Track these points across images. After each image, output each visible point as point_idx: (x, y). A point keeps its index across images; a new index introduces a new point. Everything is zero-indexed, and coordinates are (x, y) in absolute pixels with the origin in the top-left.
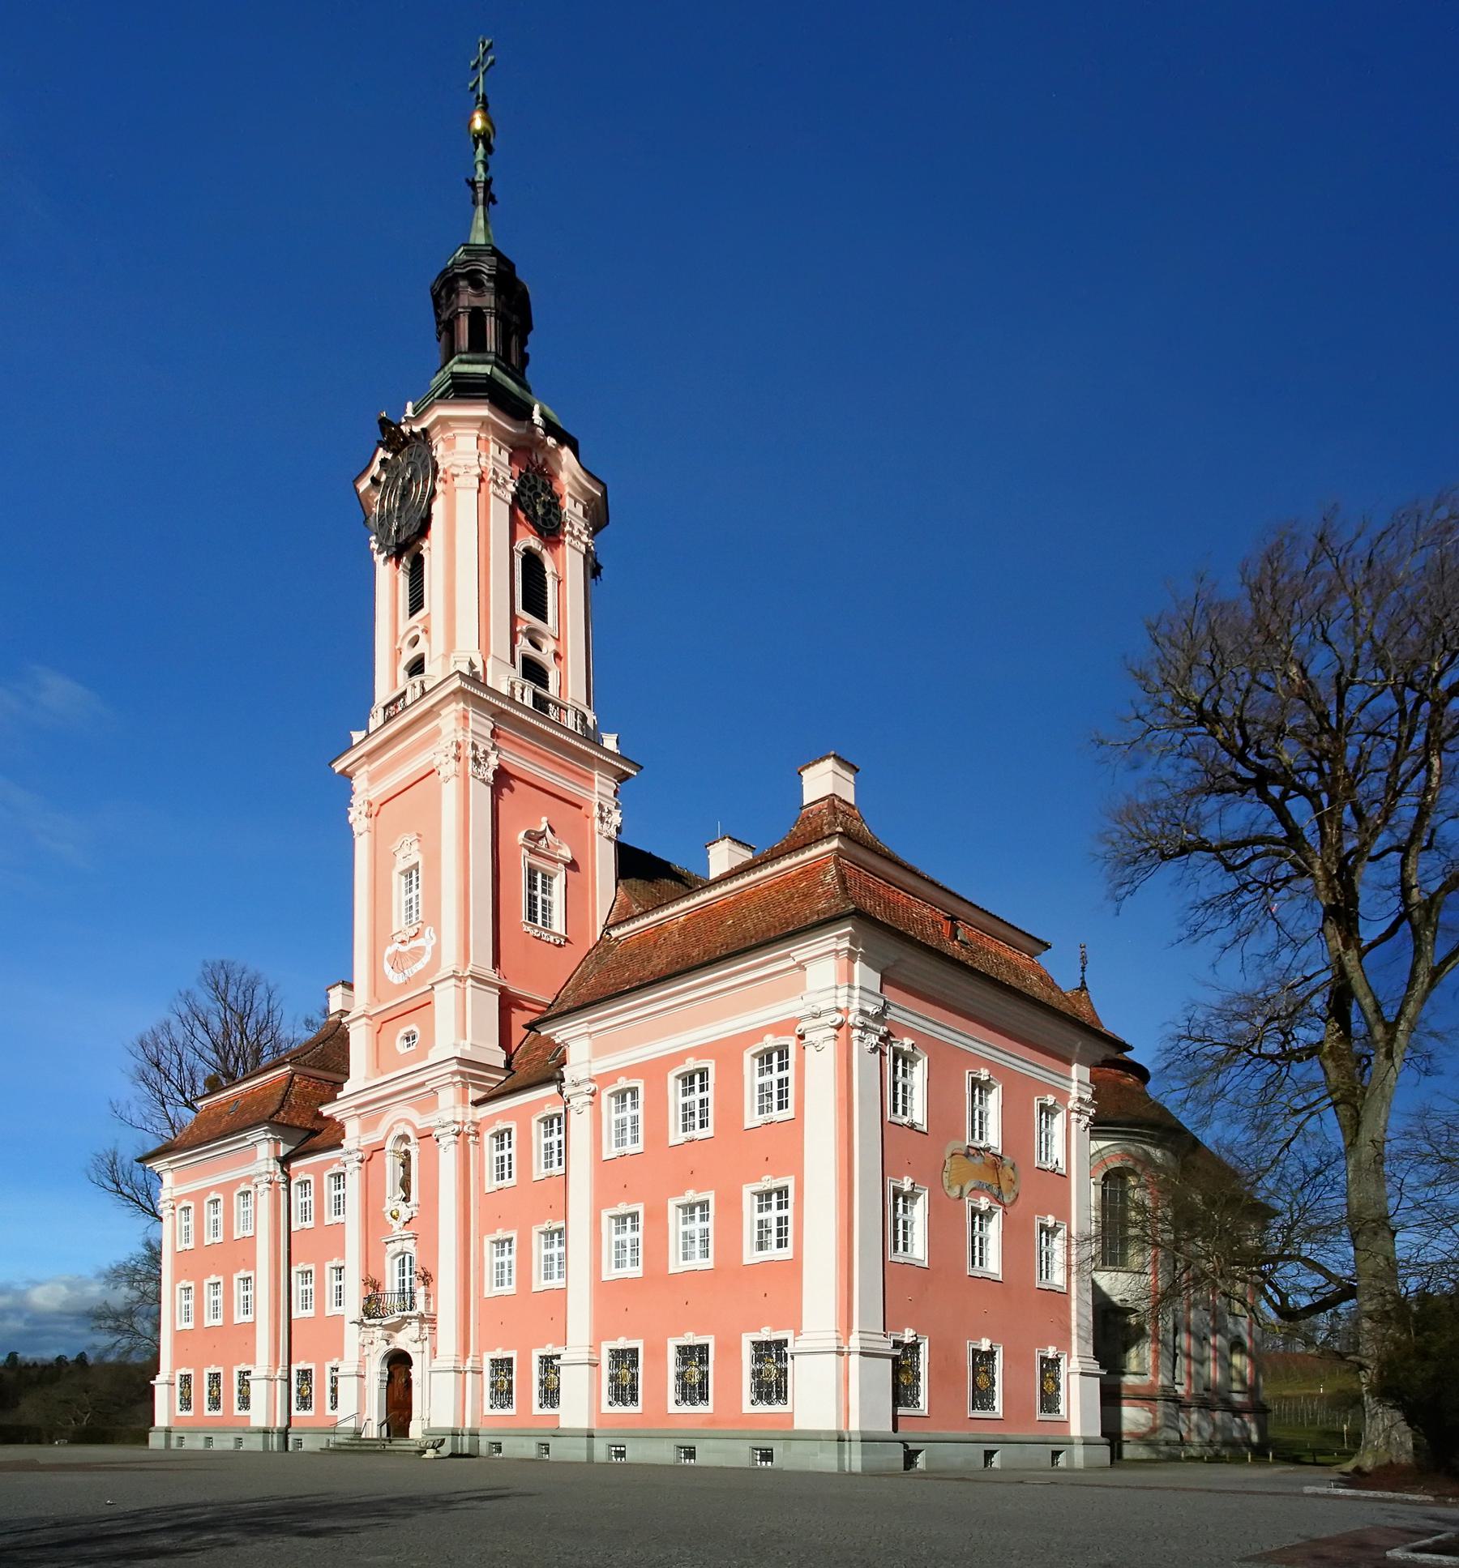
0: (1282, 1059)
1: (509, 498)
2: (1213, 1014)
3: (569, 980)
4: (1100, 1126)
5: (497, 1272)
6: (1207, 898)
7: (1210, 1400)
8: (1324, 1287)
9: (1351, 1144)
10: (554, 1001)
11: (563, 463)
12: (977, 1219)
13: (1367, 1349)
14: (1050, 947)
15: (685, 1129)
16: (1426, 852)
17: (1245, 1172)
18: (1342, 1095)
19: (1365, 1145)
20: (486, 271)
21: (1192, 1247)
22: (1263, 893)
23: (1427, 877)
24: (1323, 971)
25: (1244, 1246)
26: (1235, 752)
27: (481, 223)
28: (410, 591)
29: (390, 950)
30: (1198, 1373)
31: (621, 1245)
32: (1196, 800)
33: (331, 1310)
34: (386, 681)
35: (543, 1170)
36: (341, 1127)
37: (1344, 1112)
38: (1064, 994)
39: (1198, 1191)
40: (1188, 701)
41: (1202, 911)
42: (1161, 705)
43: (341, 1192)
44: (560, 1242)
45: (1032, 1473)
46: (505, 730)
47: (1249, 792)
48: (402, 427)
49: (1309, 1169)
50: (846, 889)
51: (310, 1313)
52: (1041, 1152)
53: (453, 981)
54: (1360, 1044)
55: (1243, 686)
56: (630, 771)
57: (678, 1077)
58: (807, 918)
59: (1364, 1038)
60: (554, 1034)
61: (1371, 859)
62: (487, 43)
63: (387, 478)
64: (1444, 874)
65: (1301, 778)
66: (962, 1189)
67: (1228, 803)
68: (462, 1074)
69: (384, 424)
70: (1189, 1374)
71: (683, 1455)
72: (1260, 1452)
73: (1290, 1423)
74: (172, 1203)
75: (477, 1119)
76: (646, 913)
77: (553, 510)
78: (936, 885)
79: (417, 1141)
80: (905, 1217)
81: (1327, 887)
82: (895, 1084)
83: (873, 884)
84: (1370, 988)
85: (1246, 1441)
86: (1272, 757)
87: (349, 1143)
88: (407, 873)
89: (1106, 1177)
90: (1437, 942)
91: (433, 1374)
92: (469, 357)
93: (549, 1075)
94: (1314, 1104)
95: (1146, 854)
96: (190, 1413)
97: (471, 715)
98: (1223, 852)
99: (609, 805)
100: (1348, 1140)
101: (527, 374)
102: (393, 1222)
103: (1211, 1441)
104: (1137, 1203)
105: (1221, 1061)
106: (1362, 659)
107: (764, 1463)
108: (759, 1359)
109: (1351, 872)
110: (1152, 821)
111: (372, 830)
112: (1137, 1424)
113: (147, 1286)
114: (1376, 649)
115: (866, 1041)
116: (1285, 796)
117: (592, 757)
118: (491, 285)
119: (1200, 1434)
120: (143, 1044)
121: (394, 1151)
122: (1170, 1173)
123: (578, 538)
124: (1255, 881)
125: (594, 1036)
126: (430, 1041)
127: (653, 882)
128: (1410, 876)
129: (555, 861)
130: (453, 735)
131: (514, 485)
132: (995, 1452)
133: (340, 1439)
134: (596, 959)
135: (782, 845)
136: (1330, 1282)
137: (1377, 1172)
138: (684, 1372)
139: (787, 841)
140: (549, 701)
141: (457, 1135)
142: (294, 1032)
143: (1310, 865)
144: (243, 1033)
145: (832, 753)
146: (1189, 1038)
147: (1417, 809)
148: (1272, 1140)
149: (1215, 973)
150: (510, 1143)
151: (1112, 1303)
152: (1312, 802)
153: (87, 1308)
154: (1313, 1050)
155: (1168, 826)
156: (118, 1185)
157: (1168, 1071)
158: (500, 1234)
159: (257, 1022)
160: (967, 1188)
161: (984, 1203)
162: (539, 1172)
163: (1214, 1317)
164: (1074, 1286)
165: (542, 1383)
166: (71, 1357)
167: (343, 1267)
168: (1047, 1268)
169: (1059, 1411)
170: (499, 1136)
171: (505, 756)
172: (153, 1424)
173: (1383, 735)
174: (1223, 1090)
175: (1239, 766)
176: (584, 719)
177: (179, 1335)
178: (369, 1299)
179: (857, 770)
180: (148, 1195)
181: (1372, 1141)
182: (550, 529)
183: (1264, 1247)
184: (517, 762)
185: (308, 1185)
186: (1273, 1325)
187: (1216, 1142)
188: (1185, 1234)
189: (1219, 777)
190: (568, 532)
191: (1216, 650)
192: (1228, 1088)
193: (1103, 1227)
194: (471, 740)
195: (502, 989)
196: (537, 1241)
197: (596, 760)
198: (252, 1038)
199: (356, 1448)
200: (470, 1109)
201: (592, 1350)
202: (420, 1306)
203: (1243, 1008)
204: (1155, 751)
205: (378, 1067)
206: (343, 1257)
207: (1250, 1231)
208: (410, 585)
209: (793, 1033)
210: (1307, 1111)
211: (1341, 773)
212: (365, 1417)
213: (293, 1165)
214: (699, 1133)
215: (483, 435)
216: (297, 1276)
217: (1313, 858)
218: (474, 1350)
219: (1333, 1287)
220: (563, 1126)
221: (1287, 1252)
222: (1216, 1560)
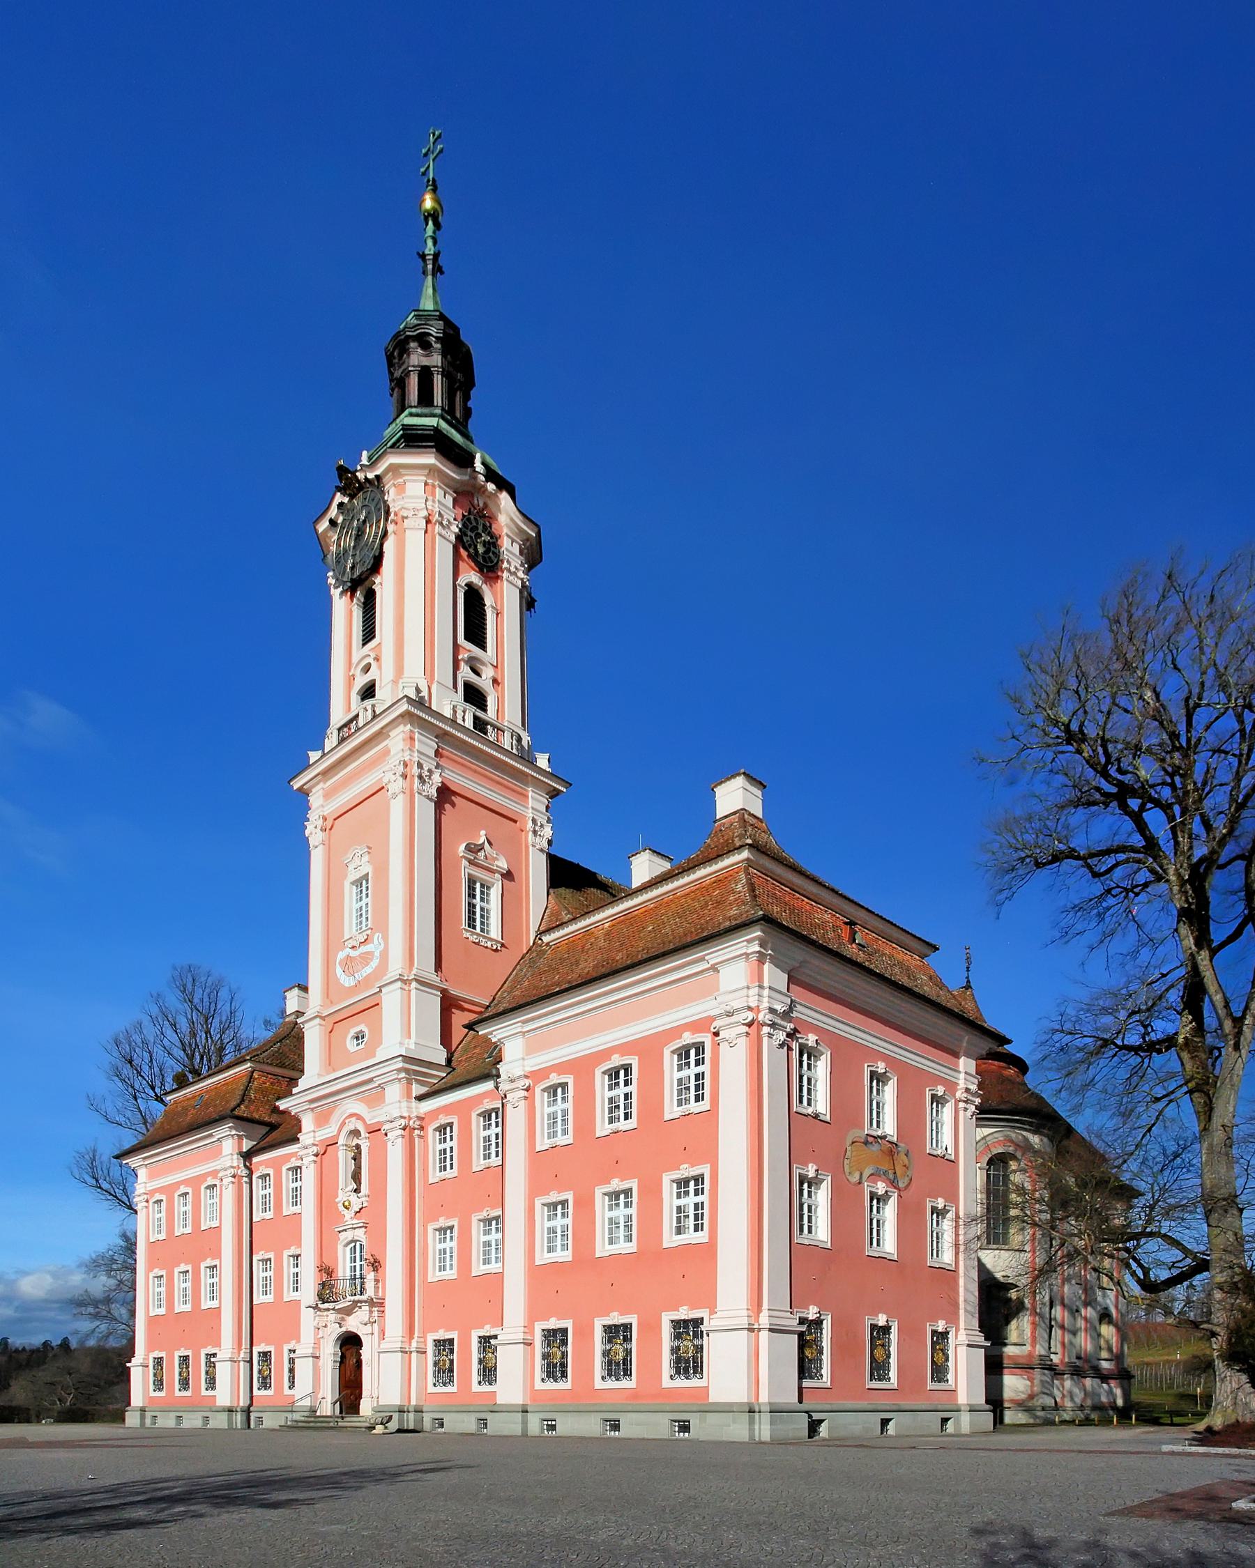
0: (1144, 1051)
1: (453, 538)
2: (1082, 1009)
3: (505, 983)
4: (986, 1113)
5: (440, 1258)
6: (1077, 902)
7: (1082, 1368)
8: (1181, 1261)
9: (1205, 1129)
10: (491, 1003)
11: (501, 507)
12: (875, 1202)
13: (1218, 1318)
14: (938, 949)
15: (611, 1122)
17: (1112, 1156)
18: (1197, 1084)
19: (1217, 1131)
20: (434, 334)
21: (1066, 1226)
22: (1126, 897)
24: (1178, 968)
25: (1111, 1224)
26: (1099, 769)
27: (430, 291)
28: (363, 622)
29: (341, 955)
30: (1071, 1343)
31: (552, 1231)
32: (1065, 812)
33: (289, 1295)
35: (482, 1162)
36: (296, 1125)
37: (1199, 1100)
39: (1071, 1174)
40: (1057, 722)
41: (1072, 914)
42: (1033, 726)
43: (298, 1184)
44: (497, 1229)
45: (923, 1439)
46: (448, 750)
47: (1111, 805)
48: (358, 474)
49: (1169, 1152)
50: (755, 896)
51: (269, 1298)
52: (932, 1139)
53: (399, 984)
54: (1213, 1037)
56: (560, 788)
57: (604, 1073)
58: (720, 924)
59: (1215, 1031)
60: (491, 1033)
62: (437, 133)
63: (344, 519)
65: (1156, 792)
66: (861, 1174)
67: (1093, 815)
68: (407, 1071)
69: (342, 471)
70: (1063, 1344)
71: (608, 1428)
72: (1124, 1415)
73: (1151, 1387)
74: (145, 1197)
77: (492, 549)
78: (837, 893)
79: (367, 1135)
80: (810, 1201)
81: (1180, 891)
82: (801, 1077)
83: (780, 892)
84: (1220, 986)
85: (1113, 1405)
86: (1131, 773)
87: (306, 1137)
88: (358, 883)
89: (990, 1162)
91: (381, 1355)
92: (419, 410)
93: (487, 1071)
94: (1172, 1092)
95: (1022, 862)
96: (162, 1394)
99: (542, 819)
100: (1202, 1125)
101: (469, 427)
103: (1082, 1406)
104: (1017, 1186)
105: (1092, 1054)
107: (682, 1434)
108: (677, 1336)
110: (1027, 832)
111: (327, 843)
112: (1016, 1391)
113: (123, 1275)
115: (774, 1037)
116: (1142, 808)
118: (439, 346)
119: (1072, 1399)
121: (346, 1145)
122: (1046, 1157)
123: (515, 574)
124: (1118, 887)
125: (527, 1036)
126: (377, 1040)
127: (581, 891)
130: (401, 754)
131: (457, 526)
132: (891, 1420)
133: (297, 1416)
134: (529, 963)
135: (697, 856)
136: (1186, 1257)
137: (1227, 1154)
139: (702, 852)
140: (486, 723)
141: (404, 1129)
142: (255, 1033)
143: (1165, 871)
145: (742, 771)
146: (1062, 1031)
148: (1136, 1126)
149: (1084, 971)
150: (451, 1136)
151: (995, 1279)
152: (1166, 813)
153: (69, 1296)
154: (1170, 1041)
155: (1041, 837)
156: (97, 1181)
157: (1044, 1063)
158: (443, 1222)
159: (221, 1022)
160: (867, 1173)
161: (881, 1188)
162: (478, 1163)
163: (1085, 1291)
164: (961, 1263)
165: (480, 1361)
166: (56, 1342)
167: (300, 1255)
168: (937, 1247)
169: (947, 1380)
170: (442, 1129)
171: (447, 774)
172: (129, 1404)
175: (1103, 781)
176: (519, 739)
177: (152, 1321)
178: (323, 1284)
179: (765, 787)
180: (125, 1190)
181: (1223, 1126)
182: (489, 566)
183: (1129, 1225)
184: (460, 780)
185: (268, 1178)
186: (1136, 1297)
188: (1060, 1214)
189: (1086, 792)
190: (506, 568)
193: (988, 1209)
194: (417, 759)
195: (444, 992)
196: (476, 1228)
197: (530, 778)
199: (312, 1424)
200: (414, 1103)
201: (526, 1330)
202: (370, 1292)
203: (1108, 1003)
205: (330, 1065)
206: (299, 1246)
207: (1117, 1210)
208: (363, 617)
209: (709, 1031)
212: (320, 1396)
213: (255, 1160)
214: (623, 1125)
215: (430, 481)
216: (258, 1264)
217: (1167, 864)
218: (419, 1332)
219: (1188, 1261)
220: (500, 1120)
221: (1148, 1230)
222: (1085, 1515)
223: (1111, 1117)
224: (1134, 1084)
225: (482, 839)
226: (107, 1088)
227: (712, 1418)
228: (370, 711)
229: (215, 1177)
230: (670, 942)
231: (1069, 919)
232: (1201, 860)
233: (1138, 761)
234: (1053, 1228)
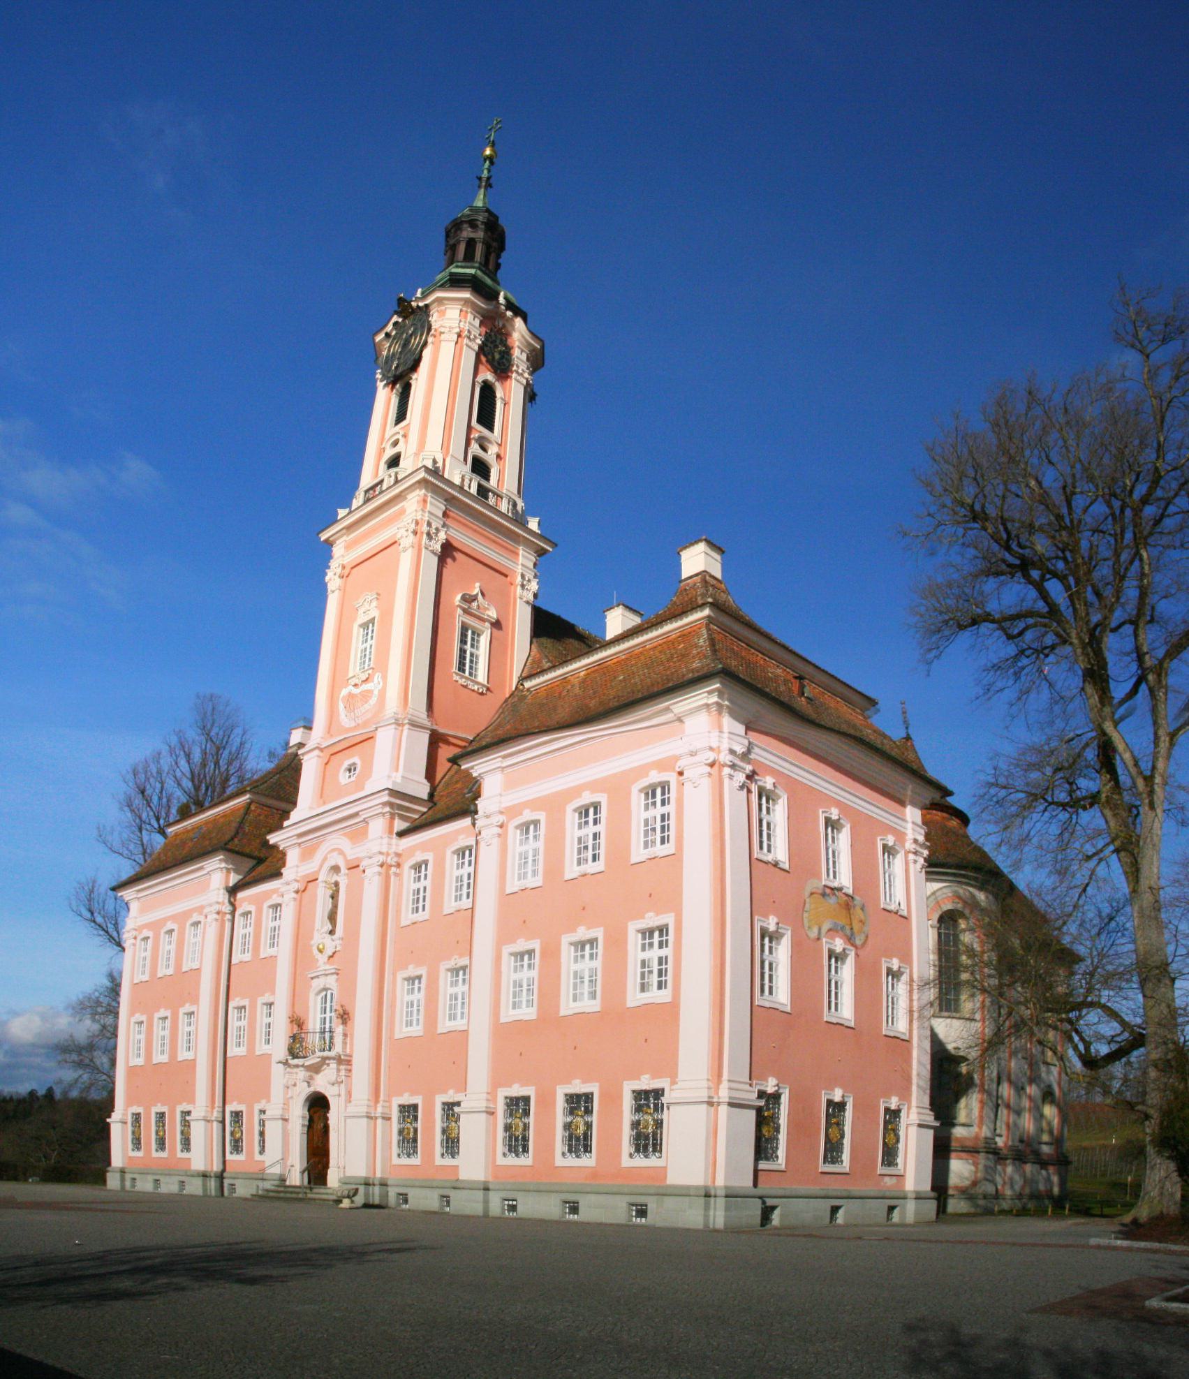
0: (1071, 807)
1: (476, 348)
2: (1012, 764)
6: (995, 661)
12: (833, 960)
16: (1150, 625)
18: (1122, 842)
21: (1013, 993)
22: (1038, 657)
23: (1157, 644)
29: (344, 692)
34: (369, 473)
35: (453, 904)
38: (894, 742)
40: (963, 503)
41: (992, 673)
42: (944, 506)
43: (276, 923)
44: (464, 980)
46: (454, 512)
49: (1104, 914)
55: (1000, 493)
61: (1114, 630)
64: (1166, 643)
66: (820, 929)
67: (1002, 584)
75: (400, 850)
76: (553, 667)
81: (1083, 653)
88: (365, 626)
89: (941, 919)
90: (1169, 702)
94: (1101, 851)
97: (429, 499)
98: (1006, 623)
99: (529, 575)
100: (1131, 886)
102: (318, 956)
104: (967, 947)
105: (1024, 807)
106: (1078, 476)
108: (638, 1109)
109: (1099, 642)
114: (1085, 469)
116: (1043, 578)
117: (518, 535)
120: (135, 773)
123: (521, 375)
124: (1030, 648)
128: (1142, 645)
129: (483, 620)
138: (571, 1123)
139: (669, 609)
140: (488, 490)
141: (381, 866)
142: (258, 763)
143: (1068, 634)
144: (217, 763)
146: (996, 785)
147: (1138, 591)
150: (426, 875)
154: (1094, 799)
155: (961, 601)
157: (984, 815)
158: (412, 971)
159: (230, 753)
160: (825, 928)
161: (839, 945)
162: (450, 905)
164: (915, 1032)
170: (417, 867)
171: (452, 533)
173: (1103, 532)
174: (1028, 835)
176: (515, 505)
182: (503, 368)
184: (463, 538)
187: (1028, 885)
188: (1007, 979)
191: (977, 467)
192: (1032, 833)
193: (940, 971)
196: (445, 978)
198: (223, 769)
200: (395, 839)
203: (1034, 759)
204: (945, 541)
210: (1096, 858)
211: (1080, 561)
213: (240, 895)
223: (1049, 876)
224: (1066, 840)
225: (476, 591)
226: (115, 817)
227: (669, 1202)
228: (393, 477)
229: (201, 913)
230: (639, 691)
231: (990, 677)
232: (1097, 626)
233: (1034, 538)
234: (1001, 995)
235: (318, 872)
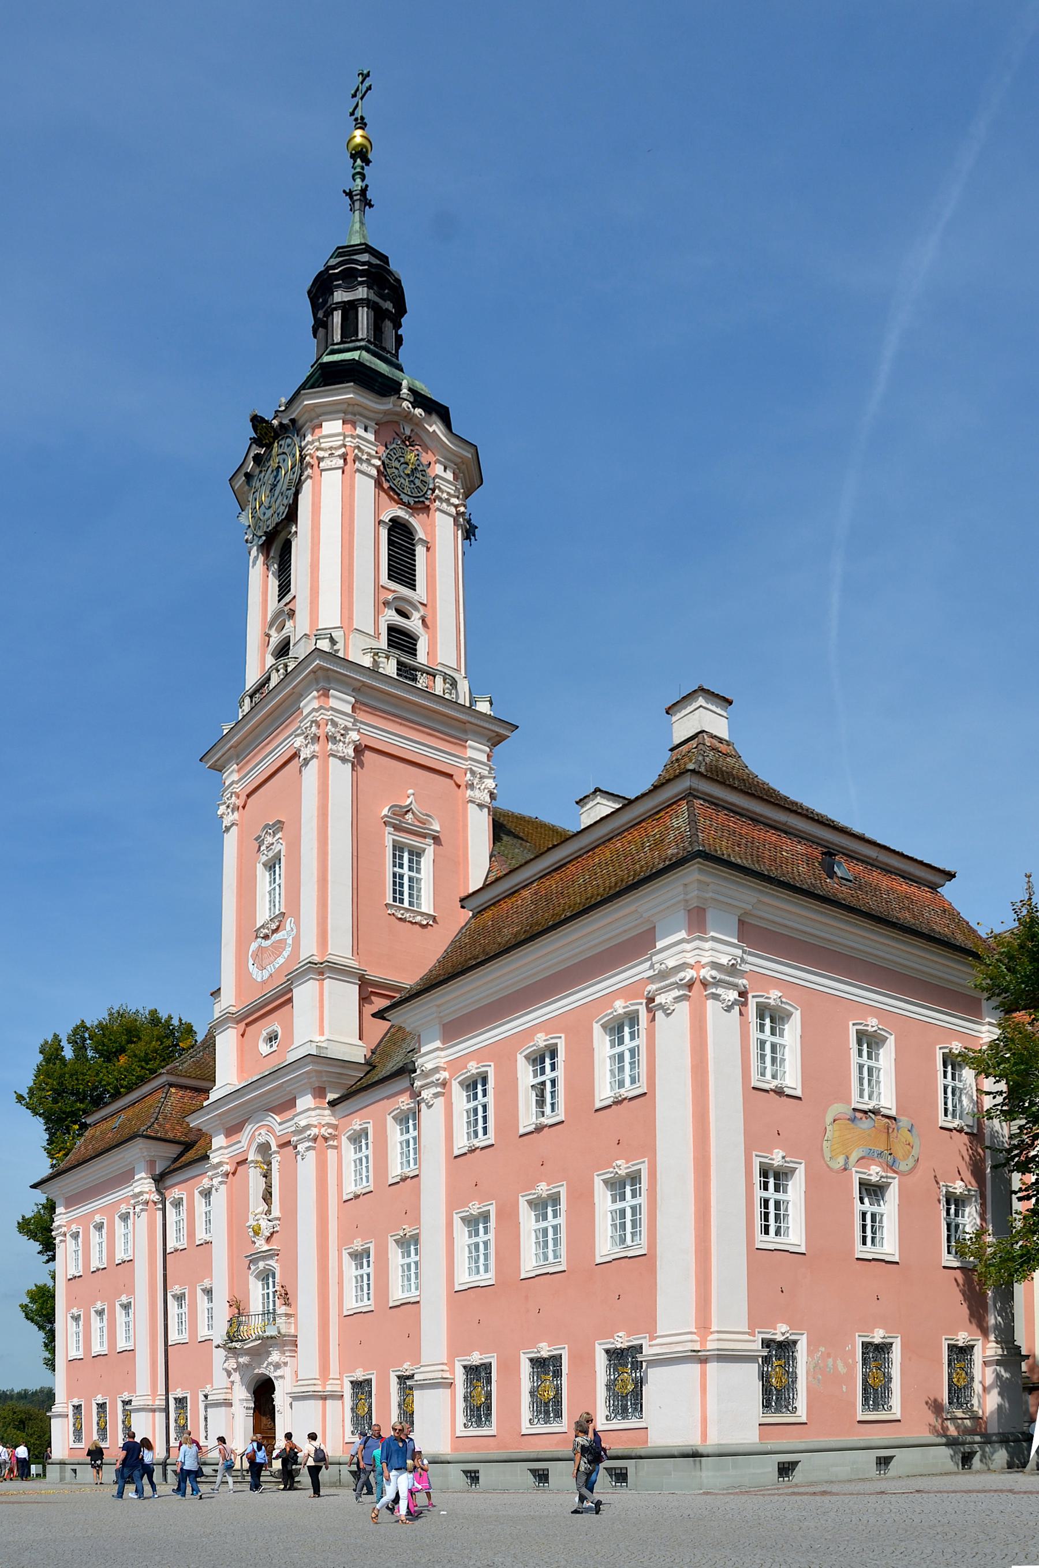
235: (247, 1151)
